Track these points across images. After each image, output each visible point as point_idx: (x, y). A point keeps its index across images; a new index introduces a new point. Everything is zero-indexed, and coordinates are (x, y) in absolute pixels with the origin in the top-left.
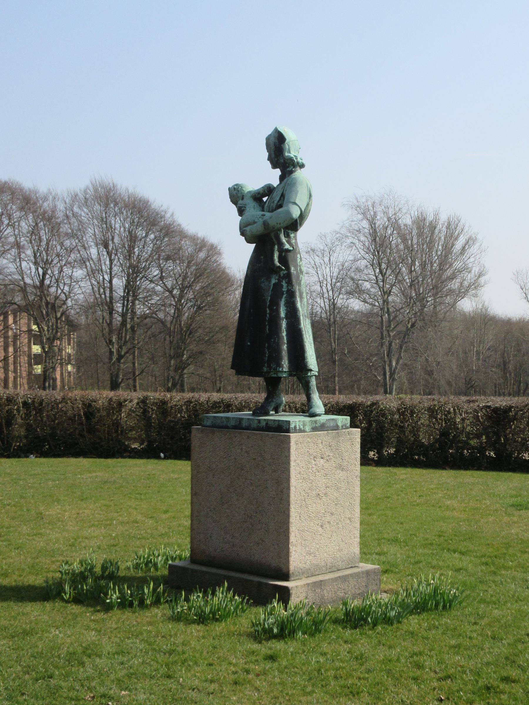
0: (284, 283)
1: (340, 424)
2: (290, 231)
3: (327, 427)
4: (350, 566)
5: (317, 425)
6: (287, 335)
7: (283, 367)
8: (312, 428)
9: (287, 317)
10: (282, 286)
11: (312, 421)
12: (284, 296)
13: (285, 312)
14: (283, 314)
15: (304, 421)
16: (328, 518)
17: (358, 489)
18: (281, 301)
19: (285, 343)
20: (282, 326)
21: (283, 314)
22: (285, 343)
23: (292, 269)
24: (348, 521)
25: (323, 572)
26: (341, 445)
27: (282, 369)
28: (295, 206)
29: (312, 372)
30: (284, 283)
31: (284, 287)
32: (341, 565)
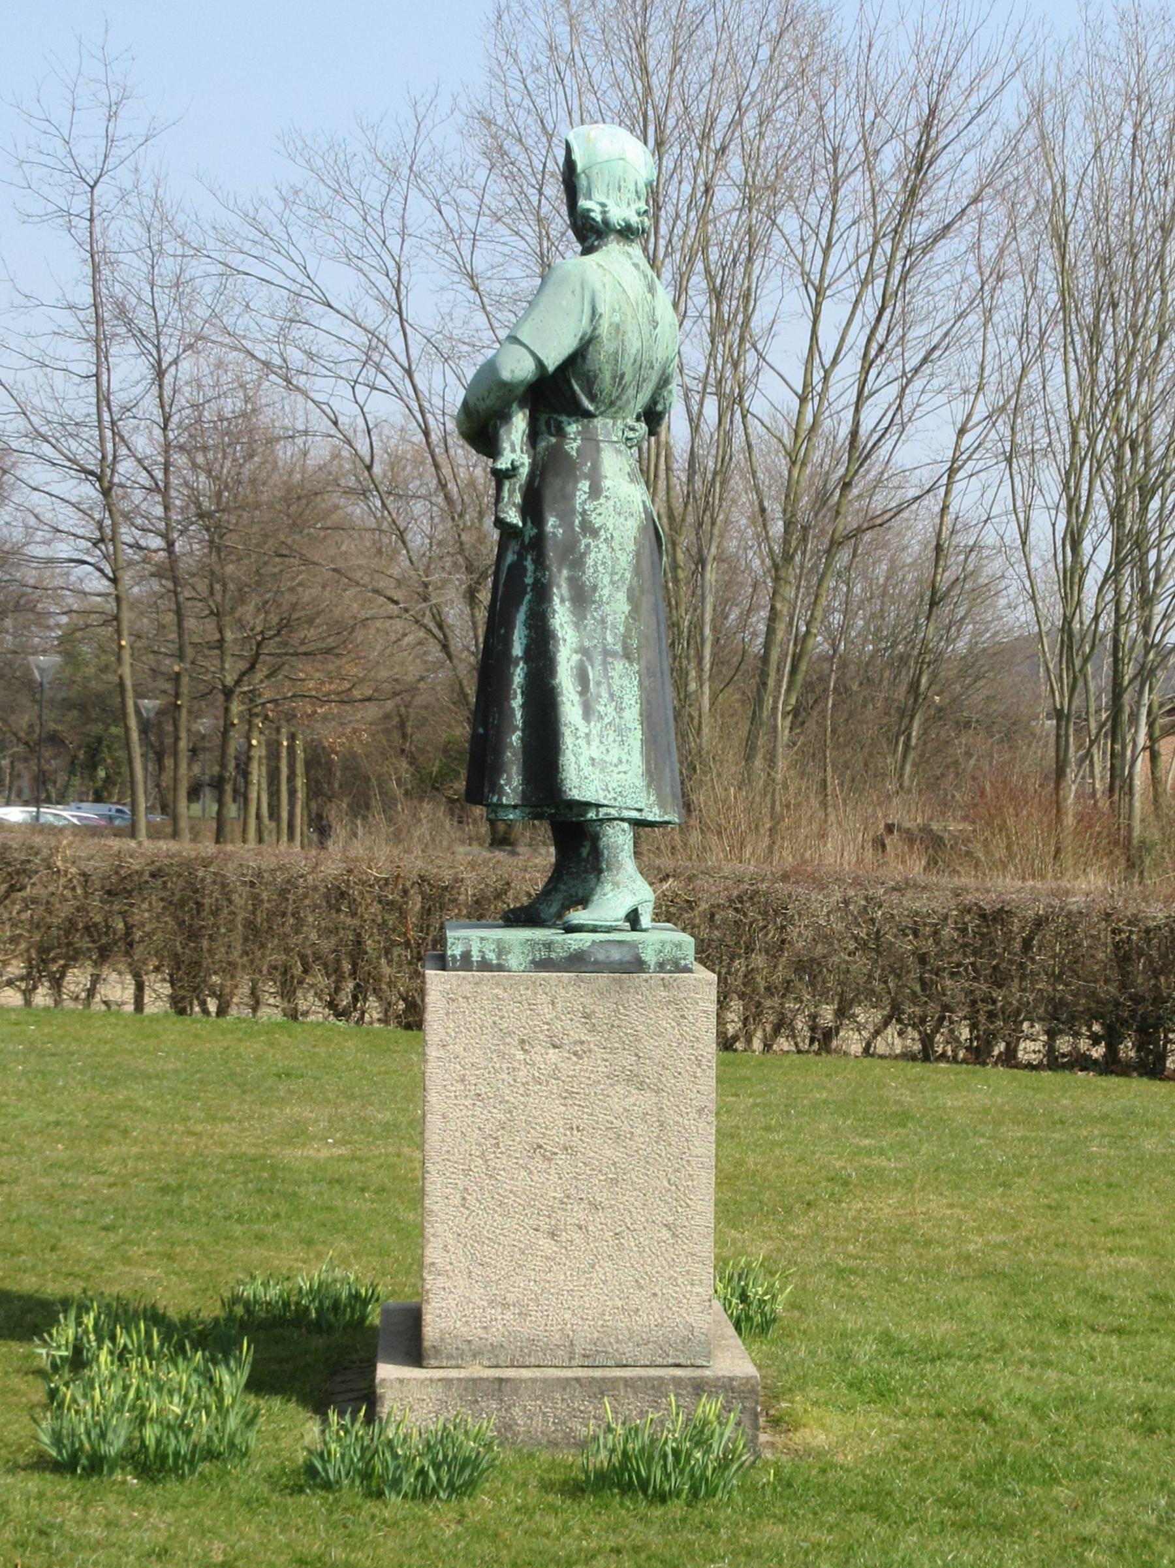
0: (529, 565)
1: (650, 957)
2: (564, 418)
3: (596, 962)
4: (671, 1361)
5: (553, 955)
6: (524, 706)
7: (501, 793)
8: (533, 962)
9: (528, 656)
10: (525, 569)
11: (532, 944)
12: (528, 597)
13: (524, 641)
14: (517, 650)
15: (499, 942)
16: (579, 1214)
17: (704, 1147)
18: (518, 610)
19: (516, 728)
20: (511, 681)
21: (517, 650)
22: (516, 728)
23: (551, 523)
24: (665, 1234)
25: (556, 1362)
26: (634, 1015)
27: (500, 799)
28: (517, 347)
29: (603, 811)
30: (529, 565)
31: (529, 574)
32: (628, 1350)
